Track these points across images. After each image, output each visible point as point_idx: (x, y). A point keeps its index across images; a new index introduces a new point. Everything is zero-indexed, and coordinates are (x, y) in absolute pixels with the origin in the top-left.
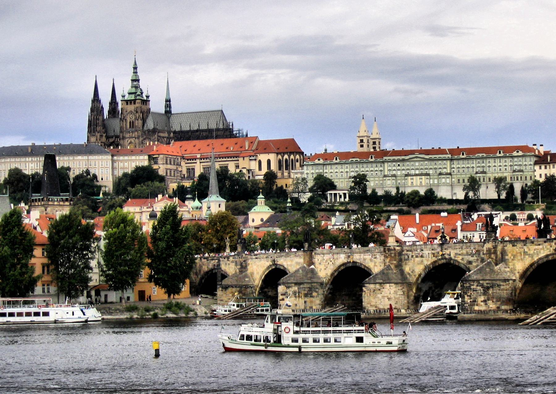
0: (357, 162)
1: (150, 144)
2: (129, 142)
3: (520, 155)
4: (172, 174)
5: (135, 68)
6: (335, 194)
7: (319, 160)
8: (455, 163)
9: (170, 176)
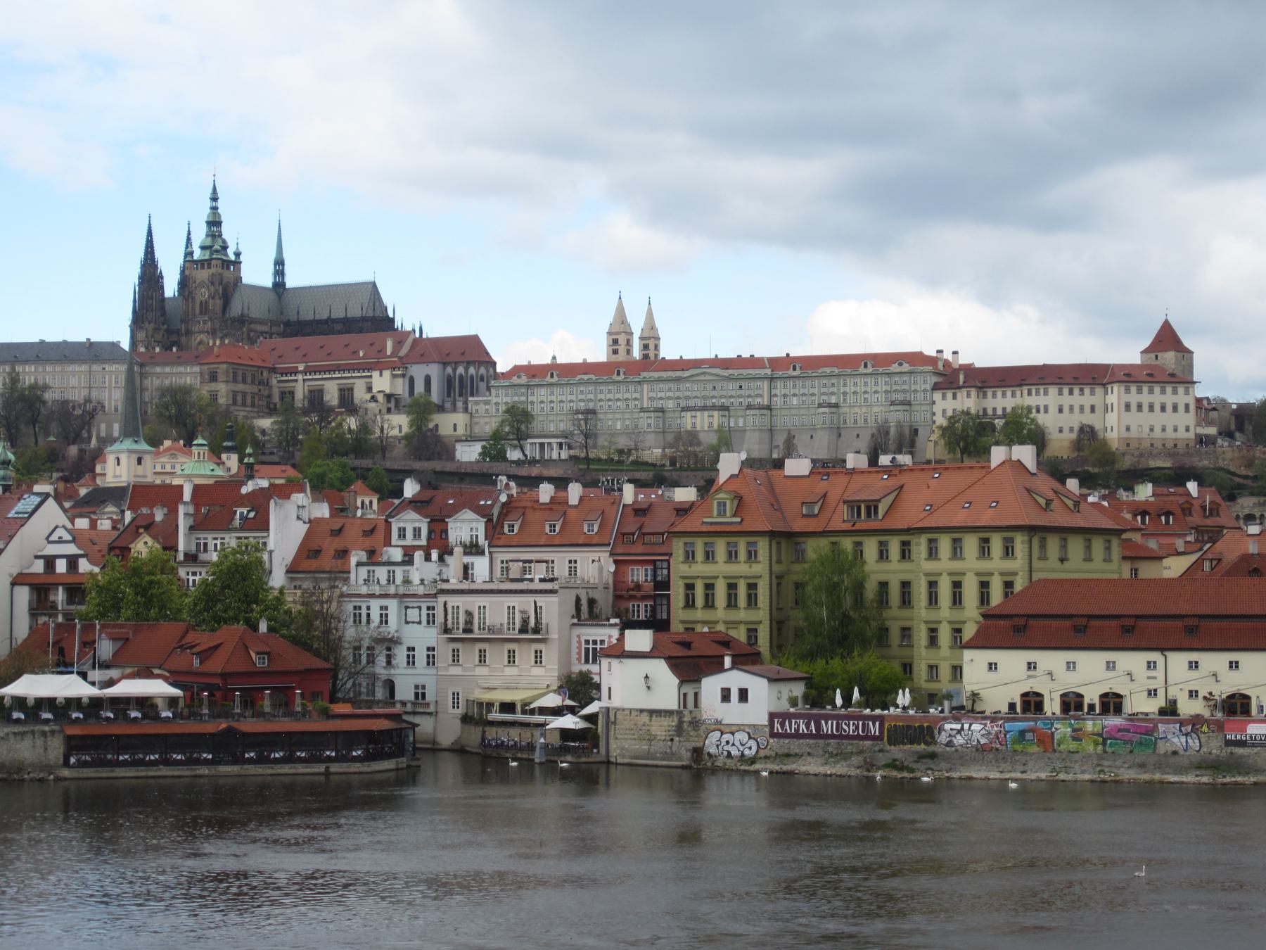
0: (589, 383)
1: (214, 344)
2: (198, 340)
3: (906, 370)
4: (249, 401)
5: (214, 198)
6: (542, 445)
7: (519, 377)
8: (779, 387)
9: (244, 404)
